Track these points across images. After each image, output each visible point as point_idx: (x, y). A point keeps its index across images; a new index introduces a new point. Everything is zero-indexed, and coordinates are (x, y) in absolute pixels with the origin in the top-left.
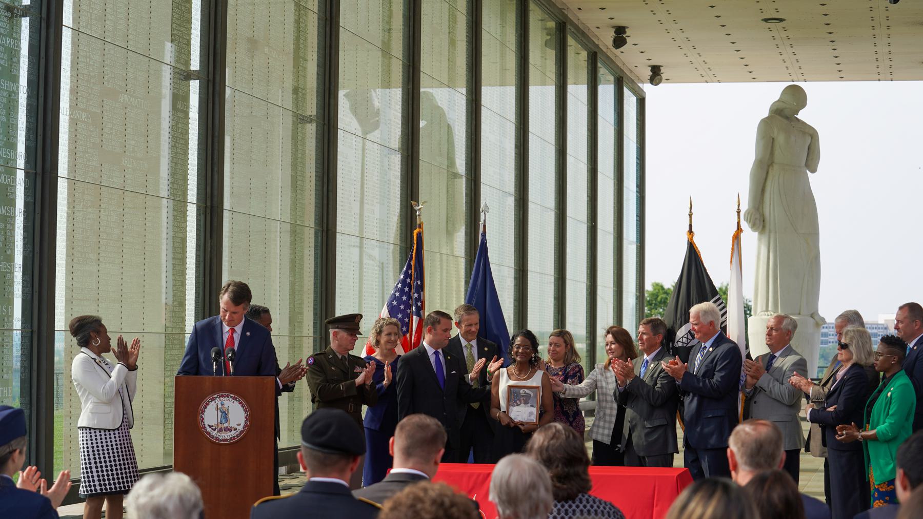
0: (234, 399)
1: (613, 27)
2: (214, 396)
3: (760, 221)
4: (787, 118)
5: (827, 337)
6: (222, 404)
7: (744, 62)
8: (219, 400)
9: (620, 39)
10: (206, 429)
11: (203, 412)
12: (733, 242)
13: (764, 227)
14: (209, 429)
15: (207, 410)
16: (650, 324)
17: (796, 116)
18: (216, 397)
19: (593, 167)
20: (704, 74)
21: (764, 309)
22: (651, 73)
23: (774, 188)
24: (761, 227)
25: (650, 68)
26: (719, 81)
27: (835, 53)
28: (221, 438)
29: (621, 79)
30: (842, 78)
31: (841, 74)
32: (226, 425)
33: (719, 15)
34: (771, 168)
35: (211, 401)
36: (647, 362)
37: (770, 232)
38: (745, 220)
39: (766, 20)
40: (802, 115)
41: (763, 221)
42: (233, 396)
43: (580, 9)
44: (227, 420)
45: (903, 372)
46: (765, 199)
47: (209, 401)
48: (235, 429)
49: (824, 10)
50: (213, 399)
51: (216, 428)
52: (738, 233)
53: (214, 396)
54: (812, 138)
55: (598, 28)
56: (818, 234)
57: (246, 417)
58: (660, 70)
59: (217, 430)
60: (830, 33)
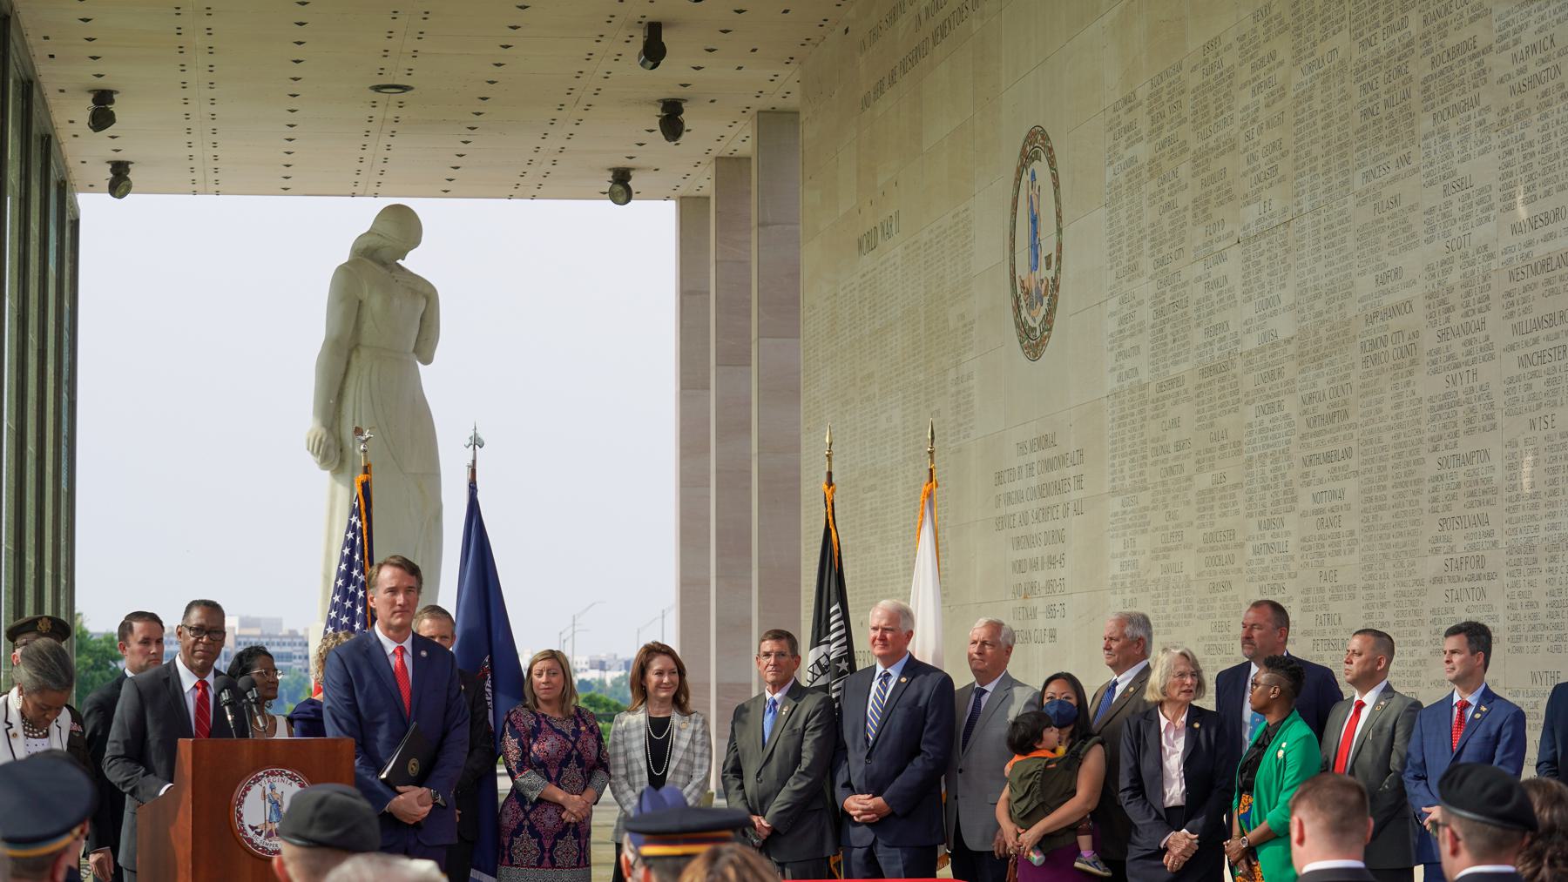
0: (292, 778)
1: (90, 91)
2: (259, 774)
3: (335, 450)
4: (384, 264)
5: (291, 661)
6: (272, 788)
7: (288, 159)
9: (102, 118)
10: (246, 834)
11: (241, 803)
12: (923, 502)
13: (342, 461)
14: (251, 833)
15: (247, 799)
16: (784, 642)
18: (262, 776)
19: (41, 348)
20: (198, 176)
22: (111, 175)
23: (361, 391)
24: (337, 462)
25: (110, 166)
26: (217, 193)
27: (462, 149)
28: (270, 848)
29: (63, 185)
30: (446, 191)
31: (448, 185)
33: (298, 77)
34: (354, 359)
35: (254, 784)
36: (775, 703)
37: (353, 470)
38: (308, 449)
39: (378, 88)
40: (412, 262)
41: (341, 450)
42: (290, 772)
43: (52, 56)
45: (1296, 713)
46: (343, 413)
49: (494, 73)
50: (257, 780)
51: (262, 831)
52: (931, 490)
53: (259, 774)
54: (428, 302)
55: (62, 91)
56: (438, 475)
58: (128, 171)
59: (264, 834)
60: (479, 114)
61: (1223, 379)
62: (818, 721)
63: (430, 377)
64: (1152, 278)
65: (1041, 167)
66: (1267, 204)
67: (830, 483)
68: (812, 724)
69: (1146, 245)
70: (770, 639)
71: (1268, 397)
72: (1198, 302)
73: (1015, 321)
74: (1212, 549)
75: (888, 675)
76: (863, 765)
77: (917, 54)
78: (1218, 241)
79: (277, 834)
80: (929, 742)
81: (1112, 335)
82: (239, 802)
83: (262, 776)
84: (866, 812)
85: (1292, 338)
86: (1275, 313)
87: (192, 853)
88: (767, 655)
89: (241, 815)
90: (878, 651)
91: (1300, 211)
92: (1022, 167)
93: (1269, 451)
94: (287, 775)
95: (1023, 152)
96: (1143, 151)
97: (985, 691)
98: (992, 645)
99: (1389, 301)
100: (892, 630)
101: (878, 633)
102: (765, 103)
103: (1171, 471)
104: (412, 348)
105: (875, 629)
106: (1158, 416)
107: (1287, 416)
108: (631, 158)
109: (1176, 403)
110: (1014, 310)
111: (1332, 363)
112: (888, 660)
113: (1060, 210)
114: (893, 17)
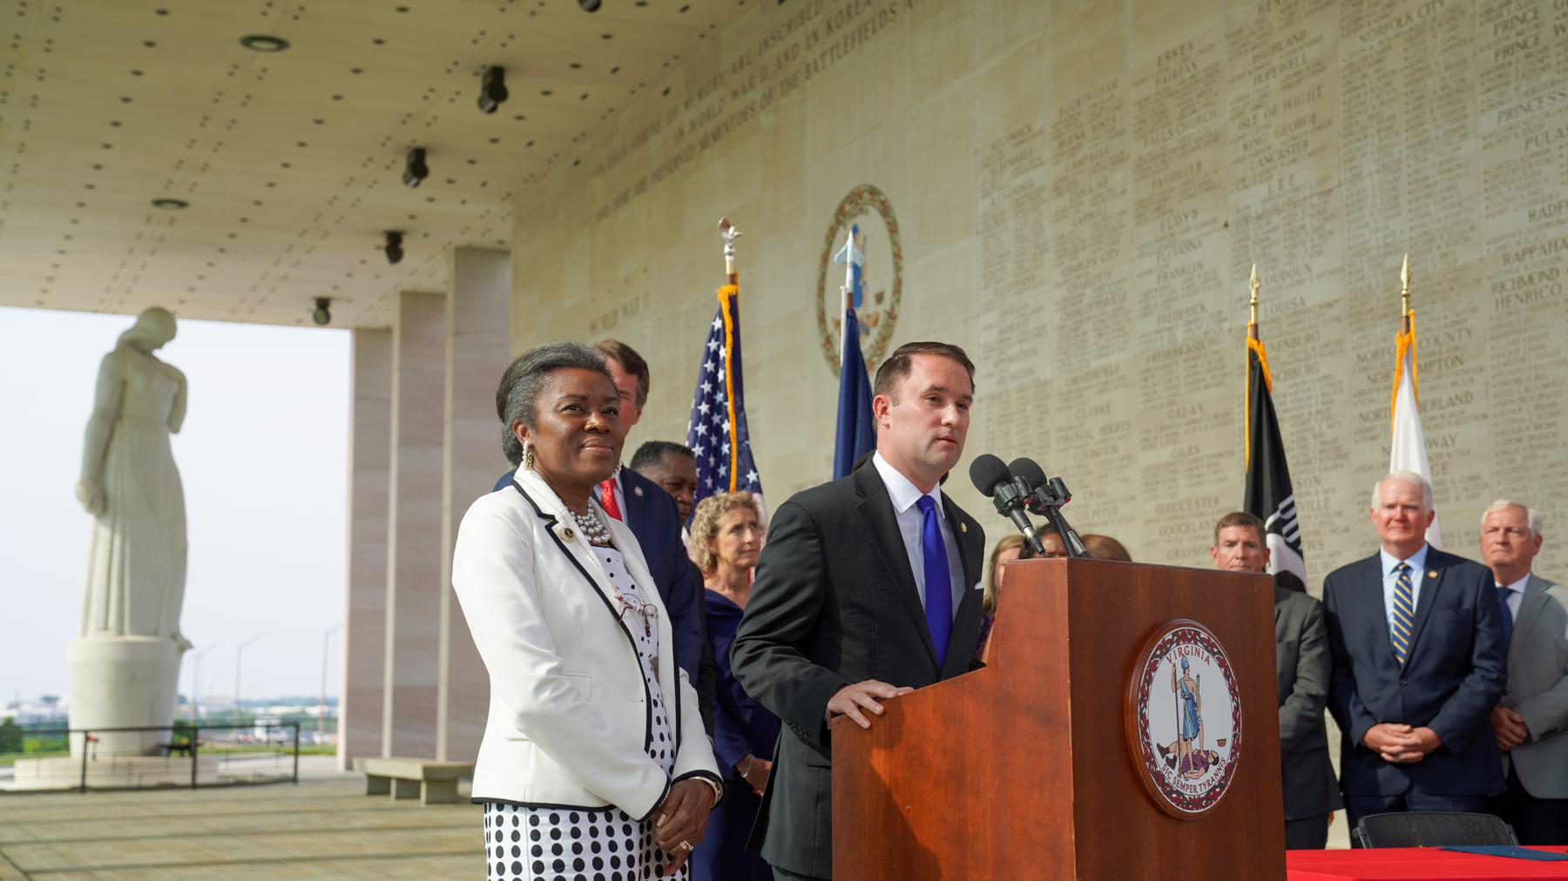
0: (1209, 647)
6: (1185, 668)
8: (1176, 649)
10: (1154, 763)
11: (1146, 694)
14: (1161, 762)
15: (1154, 690)
16: (1253, 528)
17: (157, 353)
21: (102, 626)
28: (1188, 794)
32: (1195, 745)
35: (1161, 657)
39: (158, 203)
40: (165, 354)
44: (1197, 728)
47: (1155, 655)
48: (1216, 762)
50: (1165, 649)
57: (1234, 715)
61: (1193, 359)
62: (1318, 631)
63: (182, 446)
64: (1058, 285)
65: (871, 221)
66: (1286, 183)
67: (1256, 337)
68: (1310, 634)
69: (1049, 258)
70: (1236, 524)
71: (1285, 364)
72: (1146, 293)
73: (825, 354)
74: (1175, 518)
75: (1407, 569)
76: (1397, 686)
77: (677, 162)
78: (1189, 229)
79: (1194, 764)
80: (1485, 656)
81: (987, 345)
82: (1143, 696)
83: (1171, 642)
84: (1409, 748)
85: (1337, 301)
86: (1300, 282)
87: (1075, 804)
88: (1232, 544)
89: (1147, 723)
90: (1395, 535)
91: (1358, 175)
92: (839, 222)
93: (1292, 414)
94: (1202, 640)
95: (841, 215)
96: (1044, 176)
97: (1512, 591)
98: (1521, 532)
99: (1553, 233)
100: (1414, 508)
101: (1397, 513)
102: (462, 240)
103: (1095, 453)
104: (165, 418)
105: (1391, 507)
106: (1069, 407)
107: (1326, 377)
108: (335, 288)
109: (1103, 391)
110: (824, 346)
111: (1424, 313)
112: (1406, 549)
113: (899, 250)
114: (643, 138)
